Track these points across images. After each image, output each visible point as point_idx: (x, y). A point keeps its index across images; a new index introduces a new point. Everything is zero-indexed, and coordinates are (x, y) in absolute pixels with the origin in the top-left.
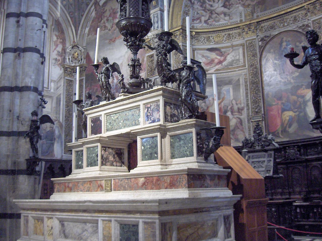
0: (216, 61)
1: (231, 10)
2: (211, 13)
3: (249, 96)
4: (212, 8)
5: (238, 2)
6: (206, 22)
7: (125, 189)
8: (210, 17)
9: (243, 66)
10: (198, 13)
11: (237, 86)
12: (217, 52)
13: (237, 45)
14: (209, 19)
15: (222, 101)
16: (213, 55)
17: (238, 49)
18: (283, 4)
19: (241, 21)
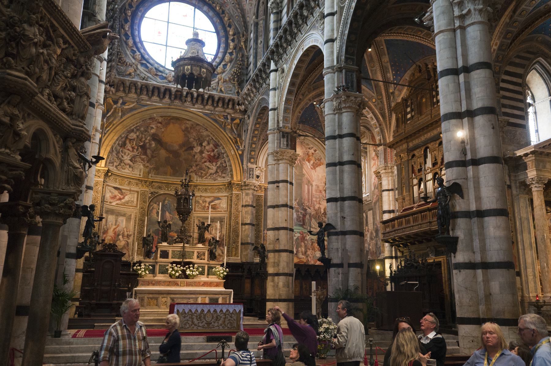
0: (118, 197)
1: (135, 165)
2: (121, 162)
3: (136, 228)
4: (122, 158)
5: (141, 161)
6: (116, 167)
7: (192, 286)
8: (119, 164)
9: (135, 207)
10: (113, 159)
11: (129, 219)
12: (119, 191)
13: (133, 191)
14: (118, 165)
15: (117, 227)
16: (116, 193)
17: (134, 194)
18: (170, 176)
19: (140, 175)
